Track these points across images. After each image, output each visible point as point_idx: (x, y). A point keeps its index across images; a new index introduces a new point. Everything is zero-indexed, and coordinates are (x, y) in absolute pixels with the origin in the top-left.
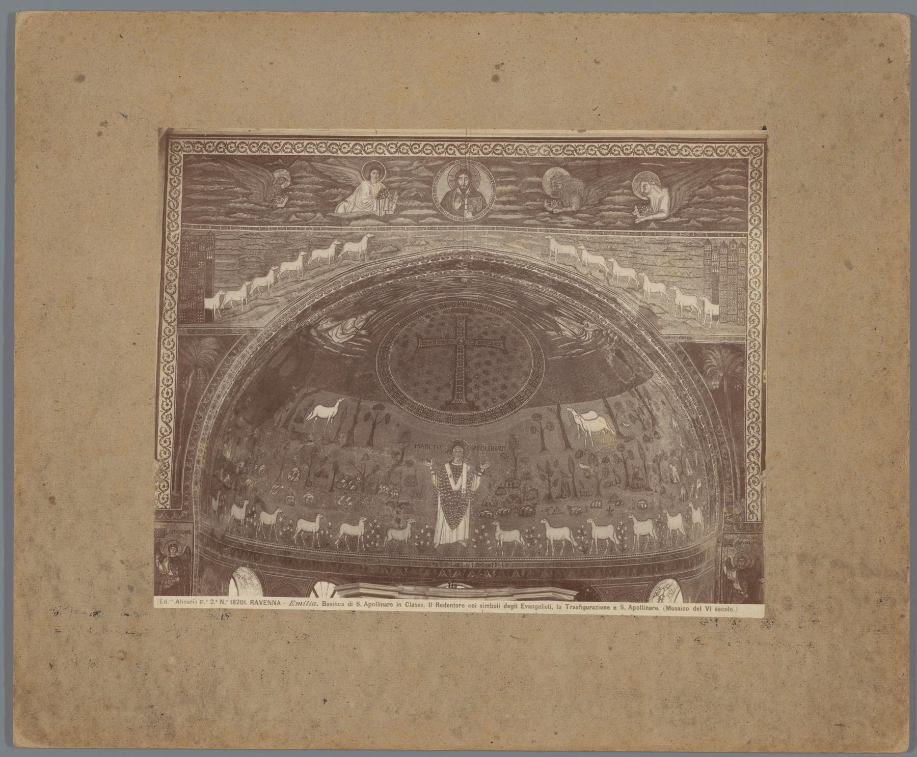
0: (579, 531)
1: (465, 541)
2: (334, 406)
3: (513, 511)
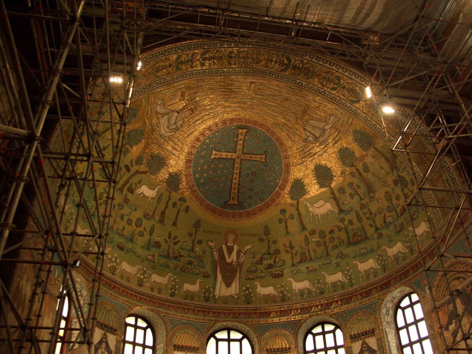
0: (316, 281)
1: (235, 295)
2: (154, 190)
3: (268, 275)
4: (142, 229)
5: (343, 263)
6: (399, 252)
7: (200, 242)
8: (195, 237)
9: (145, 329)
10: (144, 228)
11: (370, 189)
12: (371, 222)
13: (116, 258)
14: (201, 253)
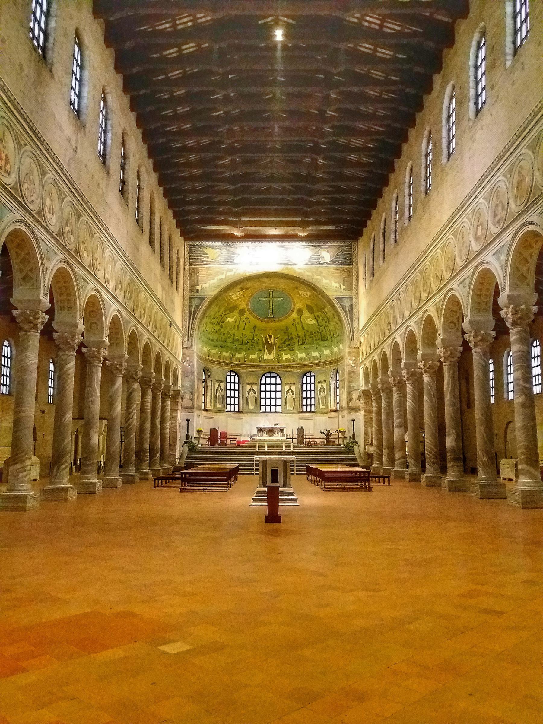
5: (319, 348)
7: (256, 335)
9: (234, 376)
11: (329, 321)
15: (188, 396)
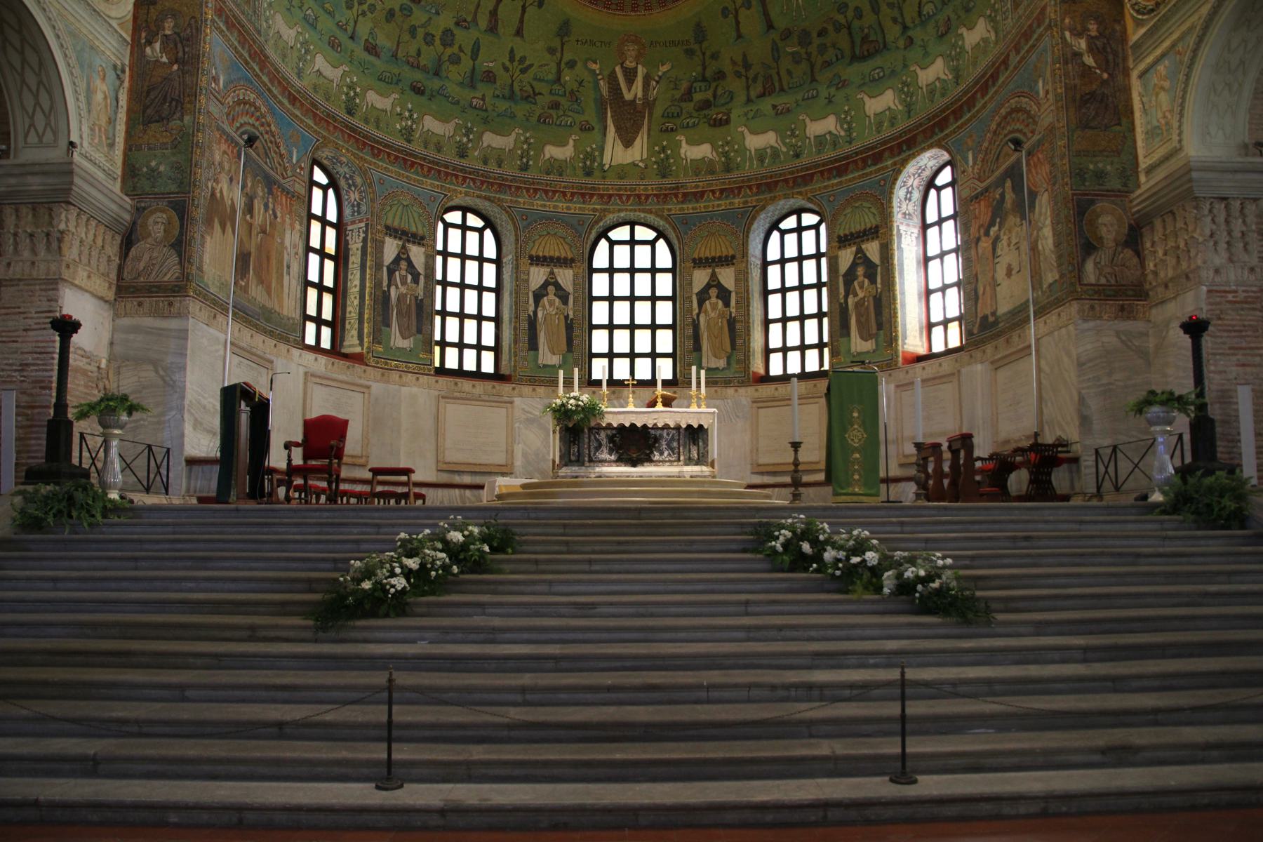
4: (455, 49)
6: (938, 79)
7: (571, 64)
8: (562, 54)
9: (480, 231)
10: (461, 49)
12: (896, 13)
13: (410, 111)
14: (575, 86)
15: (158, 224)
